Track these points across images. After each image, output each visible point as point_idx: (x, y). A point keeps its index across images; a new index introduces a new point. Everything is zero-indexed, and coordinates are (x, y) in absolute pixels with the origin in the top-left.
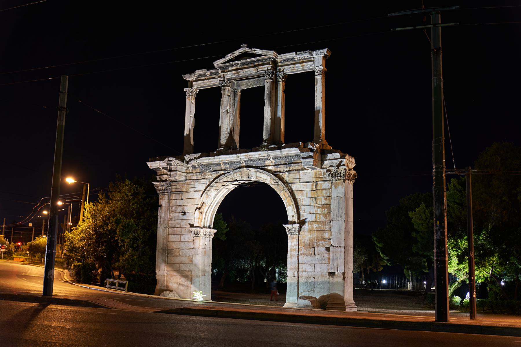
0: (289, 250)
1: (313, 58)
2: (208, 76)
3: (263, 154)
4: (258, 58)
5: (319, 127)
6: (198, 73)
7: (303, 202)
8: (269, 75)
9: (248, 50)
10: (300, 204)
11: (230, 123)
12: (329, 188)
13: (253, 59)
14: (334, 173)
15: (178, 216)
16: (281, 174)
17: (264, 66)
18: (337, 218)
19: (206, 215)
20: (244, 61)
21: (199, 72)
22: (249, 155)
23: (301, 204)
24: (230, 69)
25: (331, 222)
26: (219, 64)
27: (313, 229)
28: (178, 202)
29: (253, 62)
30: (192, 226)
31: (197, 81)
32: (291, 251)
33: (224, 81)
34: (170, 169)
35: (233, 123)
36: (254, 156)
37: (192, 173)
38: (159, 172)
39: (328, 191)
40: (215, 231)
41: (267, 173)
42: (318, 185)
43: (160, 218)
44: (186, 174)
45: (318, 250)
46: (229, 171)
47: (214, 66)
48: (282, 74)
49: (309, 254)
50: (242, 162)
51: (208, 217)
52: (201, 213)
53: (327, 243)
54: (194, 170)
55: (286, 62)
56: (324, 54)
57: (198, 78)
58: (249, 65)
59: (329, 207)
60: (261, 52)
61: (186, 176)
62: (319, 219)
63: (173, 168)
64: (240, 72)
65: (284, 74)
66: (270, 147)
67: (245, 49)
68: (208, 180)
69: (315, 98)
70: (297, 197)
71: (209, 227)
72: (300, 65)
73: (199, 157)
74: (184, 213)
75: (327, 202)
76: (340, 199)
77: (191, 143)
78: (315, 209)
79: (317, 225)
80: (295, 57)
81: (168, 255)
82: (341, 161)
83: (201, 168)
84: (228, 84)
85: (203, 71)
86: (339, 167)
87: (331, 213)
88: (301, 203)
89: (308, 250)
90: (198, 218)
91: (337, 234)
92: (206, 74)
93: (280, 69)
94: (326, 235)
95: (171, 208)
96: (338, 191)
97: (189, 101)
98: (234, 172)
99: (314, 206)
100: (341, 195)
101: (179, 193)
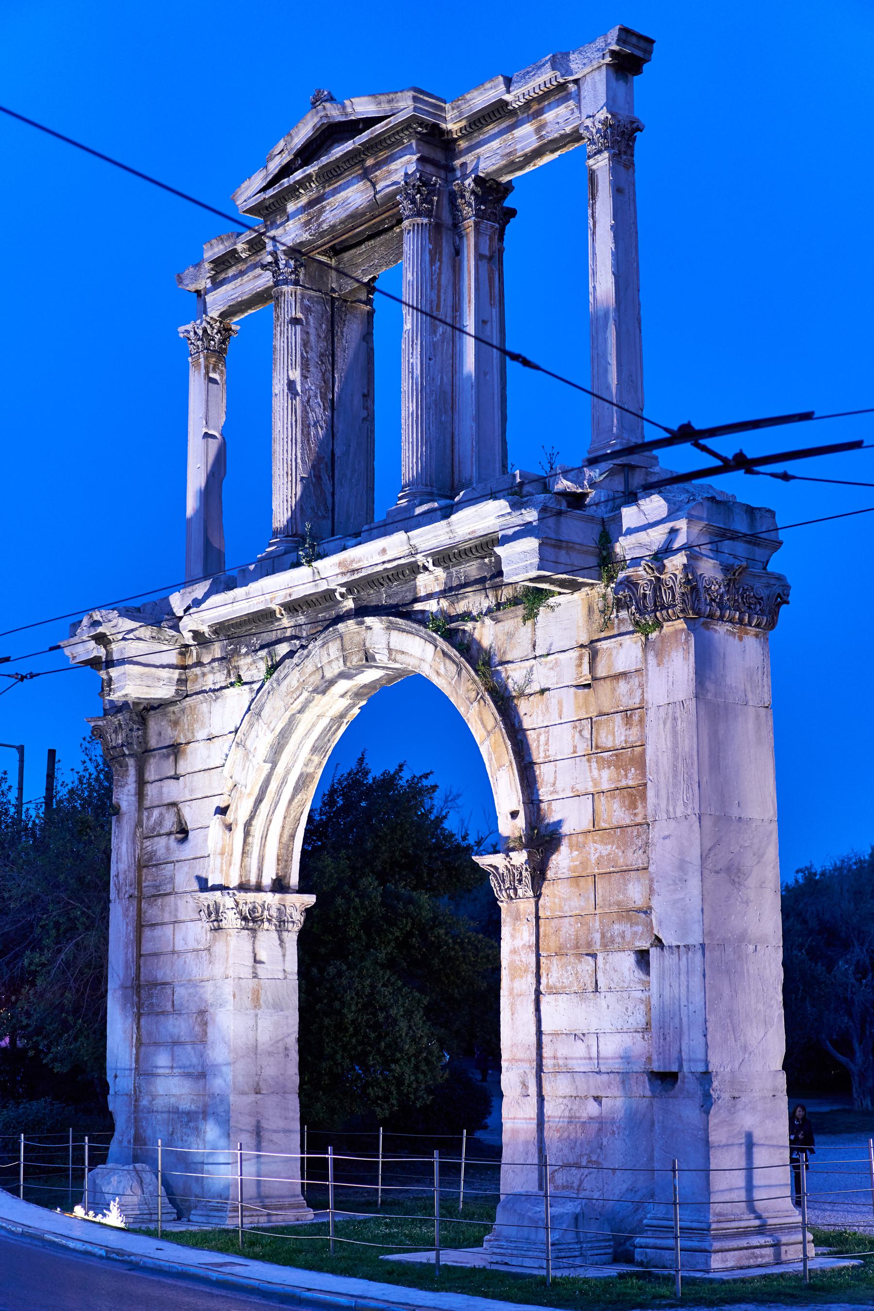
0: (504, 974)
1: (576, 82)
2: (247, 258)
7: (547, 744)
8: (414, 197)
10: (537, 755)
11: (306, 434)
12: (639, 667)
13: (349, 146)
14: (647, 592)
16: (468, 626)
17: (393, 166)
18: (671, 810)
19: (247, 834)
20: (324, 160)
23: (542, 755)
26: (250, 198)
27: (585, 868)
28: (165, 790)
29: (353, 158)
30: (204, 885)
31: (217, 284)
32: (513, 978)
33: (276, 262)
35: (326, 436)
37: (199, 664)
39: (637, 684)
40: (310, 899)
41: (421, 628)
42: (598, 659)
44: (178, 671)
45: (607, 967)
47: (238, 209)
48: (472, 185)
49: (575, 988)
50: (342, 595)
51: (263, 846)
52: (229, 827)
53: (640, 929)
54: (204, 650)
55: (481, 128)
56: (613, 53)
57: (217, 273)
59: (640, 763)
61: (181, 682)
62: (605, 816)
63: (117, 649)
64: (321, 211)
65: (478, 180)
66: (419, 510)
67: (324, 108)
68: (246, 687)
69: (590, 262)
70: (527, 723)
71: (280, 886)
72: (527, 129)
73: (207, 596)
75: (634, 734)
76: (678, 714)
78: (591, 772)
79: (605, 850)
80: (507, 97)
81: (142, 1011)
82: (673, 532)
84: (292, 273)
86: (665, 561)
87: (649, 784)
88: (542, 748)
89: (573, 967)
90: (219, 851)
91: (672, 887)
92: (235, 251)
93: (464, 165)
94: (635, 893)
95: (148, 818)
96: (671, 679)
97: (199, 373)
98: (319, 643)
99: (589, 761)
100: (681, 696)
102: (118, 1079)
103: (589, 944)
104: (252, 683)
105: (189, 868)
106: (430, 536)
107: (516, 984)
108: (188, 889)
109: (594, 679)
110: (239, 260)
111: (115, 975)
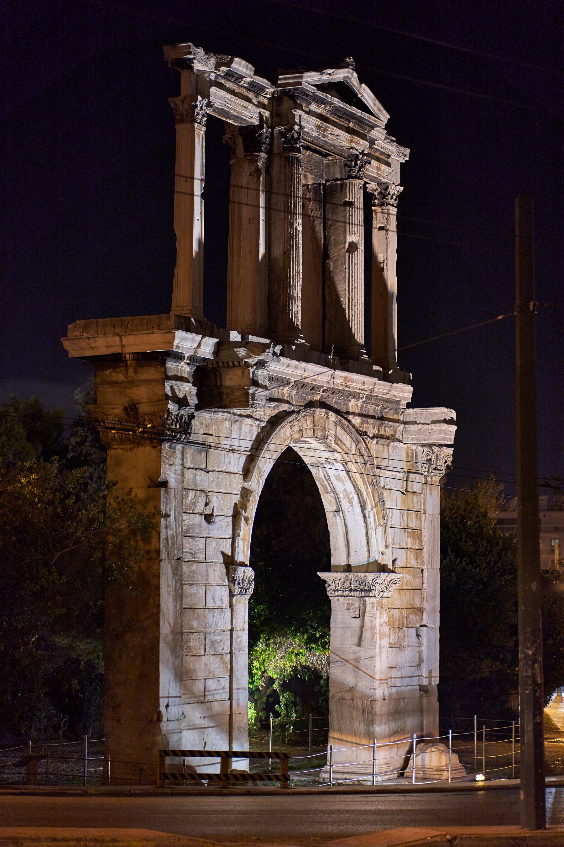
4: (366, 116)
13: (359, 112)
24: (313, 107)
25: (422, 571)
28: (198, 477)
29: (352, 116)
32: (380, 640)
60: (371, 103)
67: (352, 74)
99: (405, 531)
102: (170, 708)
105: (216, 545)
106: (383, 387)
107: (382, 642)
108: (215, 561)
109: (406, 491)
111: (166, 622)
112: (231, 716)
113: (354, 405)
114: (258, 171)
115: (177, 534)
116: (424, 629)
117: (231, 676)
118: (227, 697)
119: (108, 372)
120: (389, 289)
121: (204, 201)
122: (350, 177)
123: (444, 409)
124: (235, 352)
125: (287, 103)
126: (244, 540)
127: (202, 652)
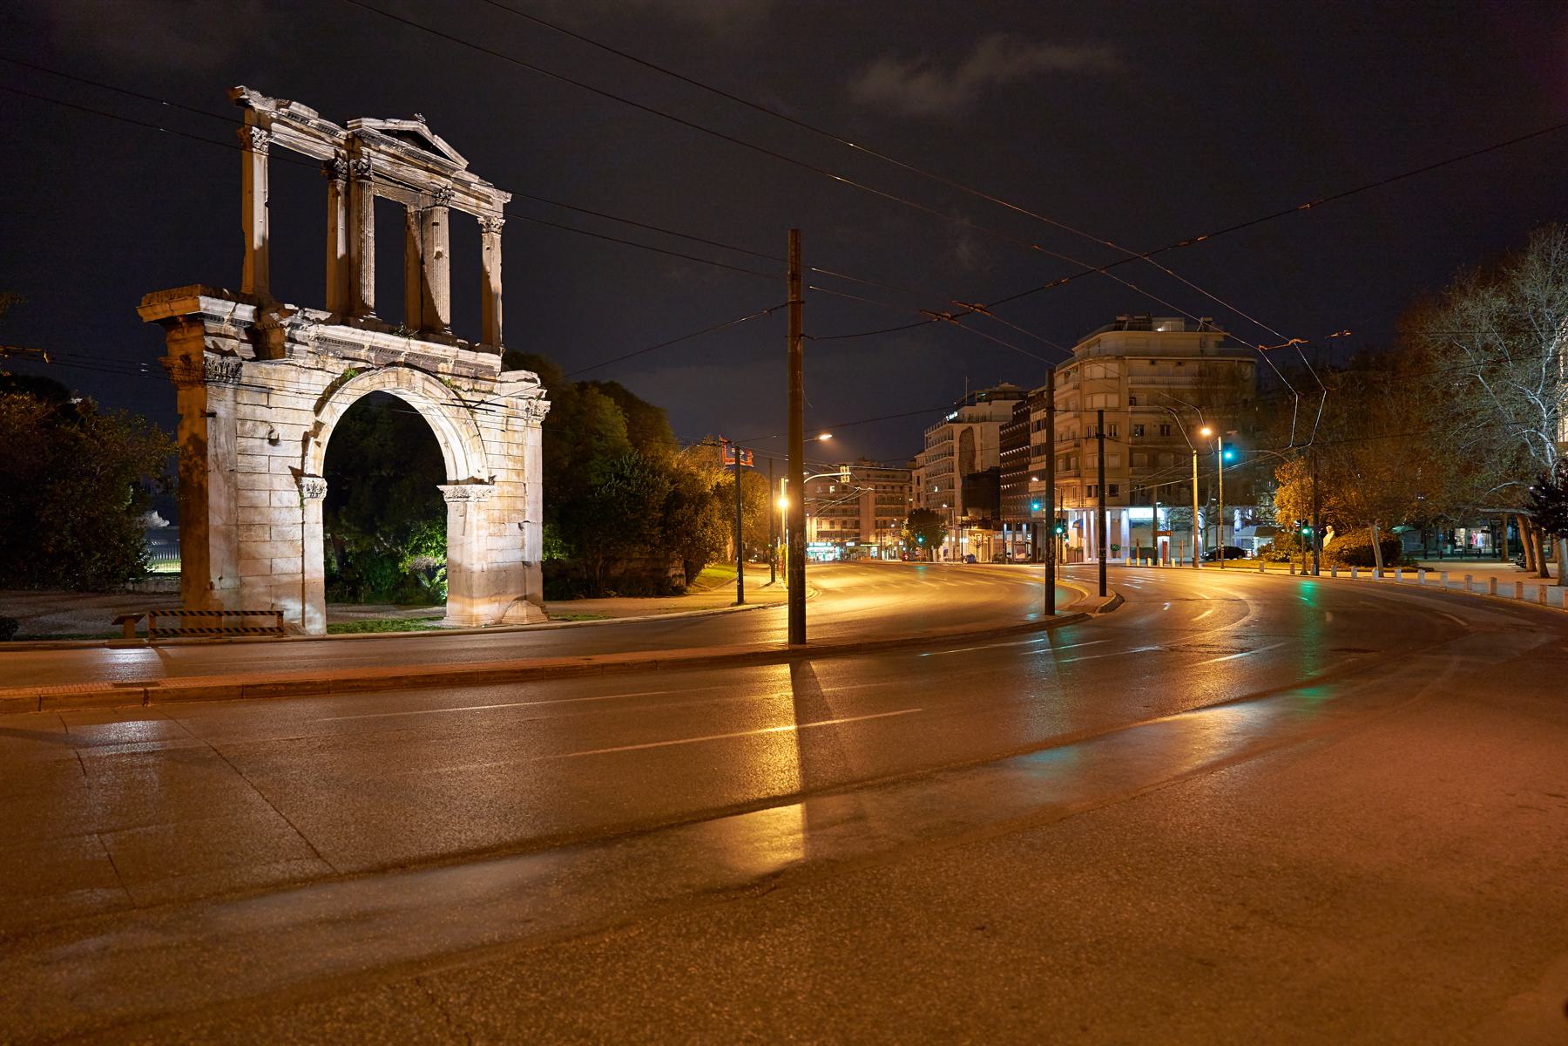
3: (436, 349)
4: (442, 159)
5: (498, 323)
6: (296, 109)
9: (425, 131)
13: (433, 156)
15: (262, 447)
17: (443, 179)
21: (299, 108)
22: (429, 348)
24: (383, 147)
25: (525, 485)
29: (428, 159)
32: (478, 529)
33: (369, 166)
34: (292, 336)
36: (432, 351)
38: (211, 326)
43: (215, 447)
46: (376, 365)
58: (419, 163)
59: (523, 462)
60: (448, 151)
66: (458, 341)
68: (330, 374)
74: (274, 442)
77: (359, 295)
79: (510, 488)
80: (473, 185)
82: (542, 392)
83: (317, 344)
85: (309, 112)
92: (308, 120)
94: (519, 505)
95: (242, 425)
101: (262, 392)
102: (223, 581)
103: (504, 520)
104: (333, 373)
109: (507, 429)
110: (306, 124)
112: (303, 584)
113: (442, 367)
114: (338, 193)
115: (229, 453)
116: (526, 524)
117: (303, 556)
118: (300, 571)
119: (173, 332)
120: (493, 290)
121: (267, 209)
122: (436, 205)
123: (524, 372)
124: (271, 317)
125: (358, 142)
126: (315, 458)
127: (269, 539)
